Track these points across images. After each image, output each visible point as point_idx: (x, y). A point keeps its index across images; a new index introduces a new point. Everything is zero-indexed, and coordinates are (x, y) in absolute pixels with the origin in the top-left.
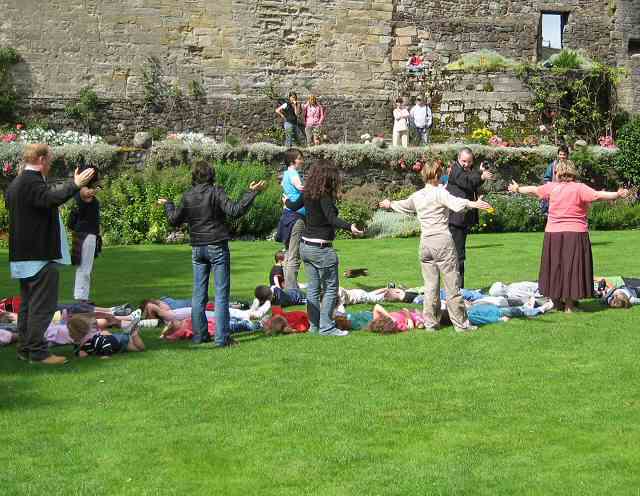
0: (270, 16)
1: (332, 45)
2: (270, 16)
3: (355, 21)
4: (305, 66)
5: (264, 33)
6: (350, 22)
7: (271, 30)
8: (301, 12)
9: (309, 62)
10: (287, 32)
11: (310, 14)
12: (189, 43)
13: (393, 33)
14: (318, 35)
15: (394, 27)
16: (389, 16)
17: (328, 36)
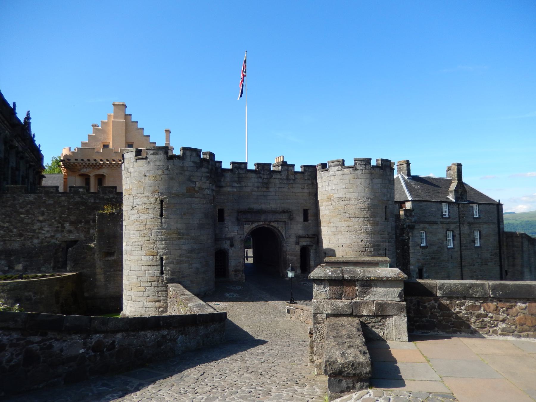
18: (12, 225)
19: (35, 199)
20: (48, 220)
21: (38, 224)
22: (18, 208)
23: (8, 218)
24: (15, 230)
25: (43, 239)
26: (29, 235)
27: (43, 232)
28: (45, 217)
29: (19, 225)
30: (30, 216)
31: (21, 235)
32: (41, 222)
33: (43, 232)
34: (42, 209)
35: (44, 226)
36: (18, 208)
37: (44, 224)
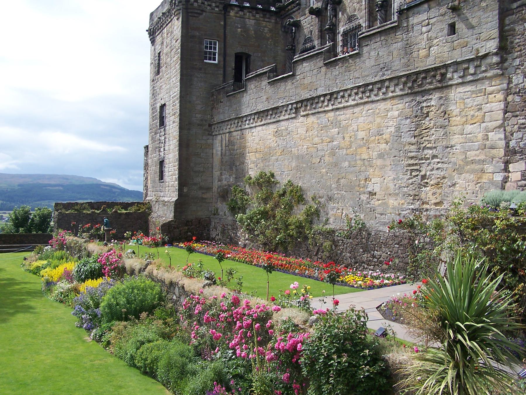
0: (413, 165)
1: (454, 185)
2: (413, 165)
3: (473, 162)
4: (436, 204)
5: (409, 179)
6: (467, 163)
7: (414, 176)
8: (432, 159)
9: (438, 201)
10: (424, 177)
11: (438, 160)
12: (369, 189)
13: (506, 170)
14: (444, 178)
15: (507, 163)
16: (502, 152)
17: (451, 177)
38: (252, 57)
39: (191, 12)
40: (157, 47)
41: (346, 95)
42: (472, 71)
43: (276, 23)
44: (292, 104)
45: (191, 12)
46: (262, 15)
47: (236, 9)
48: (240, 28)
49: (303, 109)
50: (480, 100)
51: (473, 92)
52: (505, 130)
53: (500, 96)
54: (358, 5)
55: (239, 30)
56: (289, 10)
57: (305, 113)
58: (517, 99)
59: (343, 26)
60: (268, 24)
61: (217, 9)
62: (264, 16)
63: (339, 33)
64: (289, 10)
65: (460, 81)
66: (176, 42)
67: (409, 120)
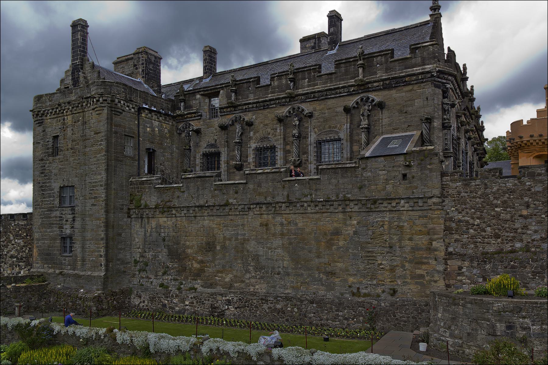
18: (484, 222)
19: (515, 185)
20: (535, 215)
21: (521, 221)
22: (492, 198)
23: (479, 213)
24: (489, 229)
25: (529, 242)
26: (507, 237)
27: (529, 232)
28: (530, 211)
29: (494, 221)
30: (508, 209)
31: (497, 236)
32: (526, 217)
33: (529, 232)
34: (526, 199)
35: (530, 224)
36: (492, 198)
37: (528, 220)
38: (157, 153)
39: (115, 111)
40: (47, 130)
41: (306, 205)
42: (420, 204)
43: (173, 125)
44: (246, 205)
45: (115, 111)
46: (164, 118)
47: (146, 111)
48: (149, 127)
49: (258, 209)
50: (425, 221)
51: (420, 217)
52: (444, 241)
53: (442, 221)
54: (272, 131)
55: (148, 129)
56: (187, 117)
57: (258, 213)
58: (454, 225)
59: (255, 143)
60: (167, 126)
61: (133, 110)
62: (165, 120)
63: (250, 147)
64: (187, 117)
65: (411, 209)
66: (97, 133)
67: (365, 228)
